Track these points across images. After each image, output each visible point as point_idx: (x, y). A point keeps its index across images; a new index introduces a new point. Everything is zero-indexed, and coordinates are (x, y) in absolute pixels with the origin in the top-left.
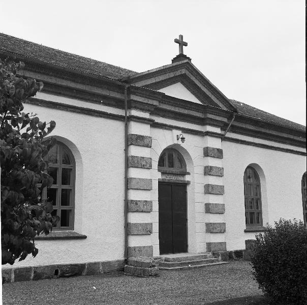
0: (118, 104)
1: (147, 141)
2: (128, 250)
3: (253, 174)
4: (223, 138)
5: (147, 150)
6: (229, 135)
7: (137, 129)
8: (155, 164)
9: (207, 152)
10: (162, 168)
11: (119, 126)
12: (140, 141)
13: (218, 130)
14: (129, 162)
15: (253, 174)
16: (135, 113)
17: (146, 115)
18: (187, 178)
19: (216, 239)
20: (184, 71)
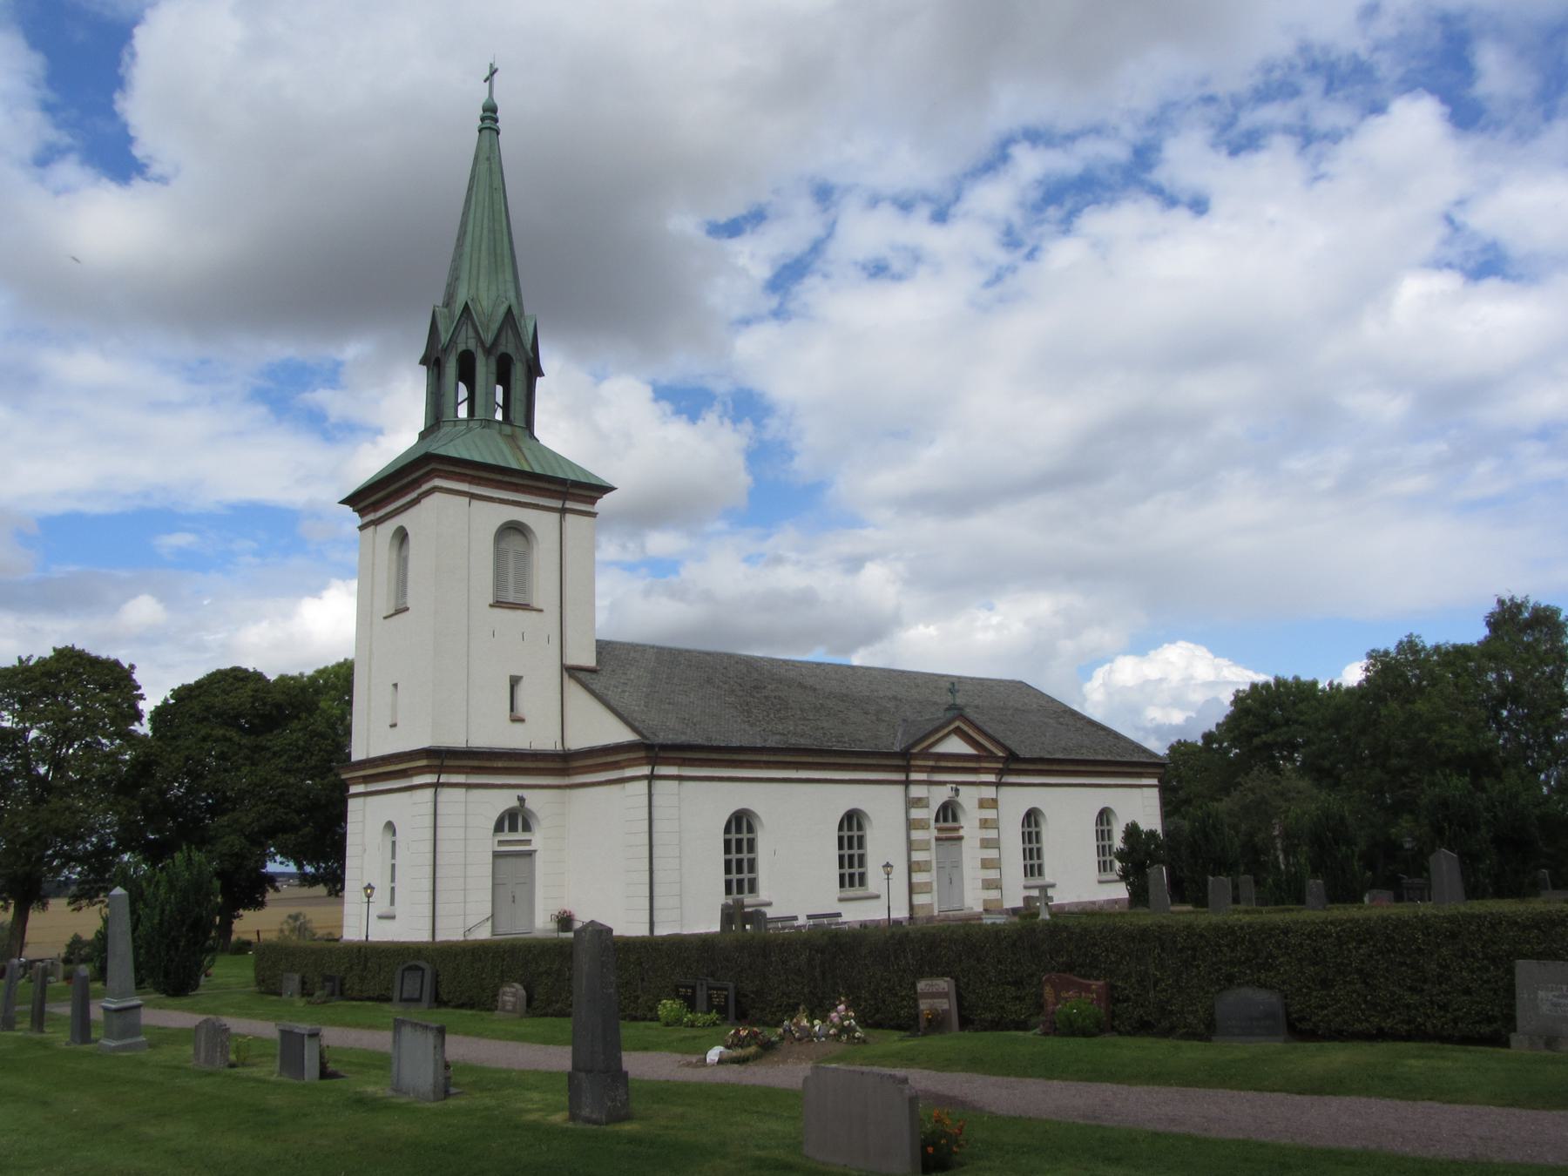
0: (896, 769)
2: (911, 907)
3: (1032, 818)
4: (998, 785)
5: (925, 811)
7: (917, 791)
8: (932, 822)
9: (983, 804)
11: (901, 788)
13: (992, 778)
14: (911, 825)
15: (1032, 818)
16: (914, 776)
18: (962, 833)
19: (993, 894)
20: (957, 723)
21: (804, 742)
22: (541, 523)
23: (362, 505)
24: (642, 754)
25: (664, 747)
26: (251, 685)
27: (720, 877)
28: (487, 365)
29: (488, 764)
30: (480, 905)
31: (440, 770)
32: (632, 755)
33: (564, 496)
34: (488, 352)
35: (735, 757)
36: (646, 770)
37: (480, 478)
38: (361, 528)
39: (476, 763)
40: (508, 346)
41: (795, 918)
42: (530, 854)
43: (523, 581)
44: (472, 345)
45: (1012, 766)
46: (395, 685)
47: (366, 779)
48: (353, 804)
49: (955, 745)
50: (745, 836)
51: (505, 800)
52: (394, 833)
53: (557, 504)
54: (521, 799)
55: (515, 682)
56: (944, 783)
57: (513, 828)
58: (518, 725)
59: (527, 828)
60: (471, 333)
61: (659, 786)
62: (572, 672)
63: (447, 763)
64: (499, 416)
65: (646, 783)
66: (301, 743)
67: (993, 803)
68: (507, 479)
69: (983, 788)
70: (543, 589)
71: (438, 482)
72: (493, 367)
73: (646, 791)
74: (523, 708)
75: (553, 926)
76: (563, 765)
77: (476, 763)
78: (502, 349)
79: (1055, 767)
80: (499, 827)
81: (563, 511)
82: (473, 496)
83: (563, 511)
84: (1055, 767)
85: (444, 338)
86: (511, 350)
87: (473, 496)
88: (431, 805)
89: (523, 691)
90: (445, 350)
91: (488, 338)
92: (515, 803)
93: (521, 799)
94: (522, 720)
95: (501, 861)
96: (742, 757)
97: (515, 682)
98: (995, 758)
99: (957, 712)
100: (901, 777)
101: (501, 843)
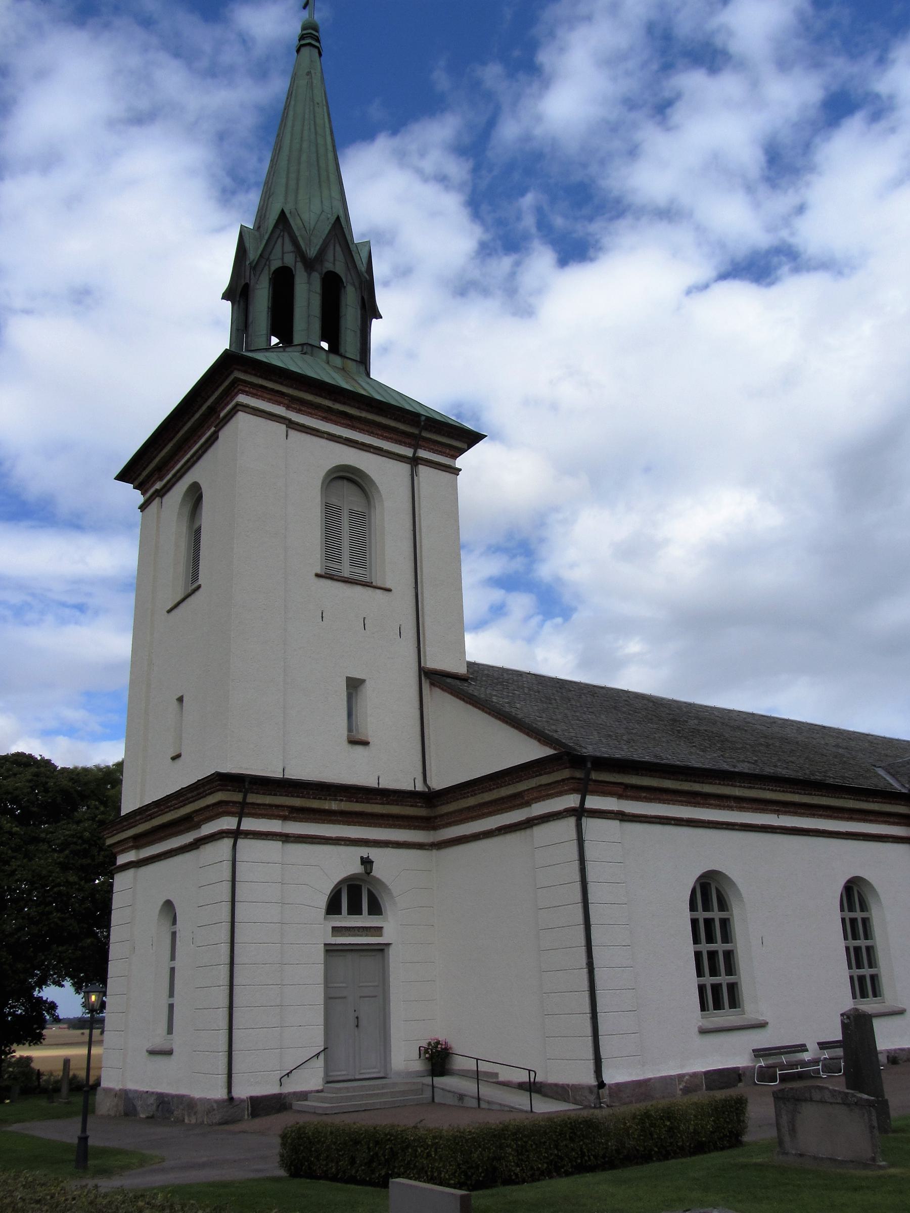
22: (386, 474)
23: (141, 478)
24: (566, 773)
25: (602, 764)
26: (34, 770)
27: (691, 981)
28: (309, 283)
29: (315, 804)
30: (306, 1029)
31: (243, 810)
32: (545, 779)
33: (415, 442)
34: (310, 265)
35: (697, 787)
36: (571, 801)
38: (143, 507)
39: (297, 802)
40: (336, 263)
41: (802, 1048)
42: (382, 949)
44: (290, 260)
46: (180, 700)
47: (139, 841)
48: (122, 882)
50: (716, 915)
51: (342, 863)
52: (174, 922)
54: (367, 862)
55: (354, 685)
57: (355, 909)
58: (359, 749)
59: (375, 908)
60: (289, 247)
61: (591, 825)
62: (434, 678)
63: (252, 798)
65: (571, 821)
66: (87, 834)
71: (242, 398)
72: (317, 285)
73: (573, 835)
74: (371, 727)
75: (418, 1065)
76: (429, 812)
77: (297, 802)
78: (328, 266)
80: (333, 907)
81: (415, 462)
82: (291, 425)
83: (415, 462)
85: (253, 255)
86: (339, 268)
88: (227, 866)
89: (370, 695)
90: (254, 268)
91: (312, 252)
92: (356, 868)
93: (367, 862)
94: (365, 743)
101: (336, 931)
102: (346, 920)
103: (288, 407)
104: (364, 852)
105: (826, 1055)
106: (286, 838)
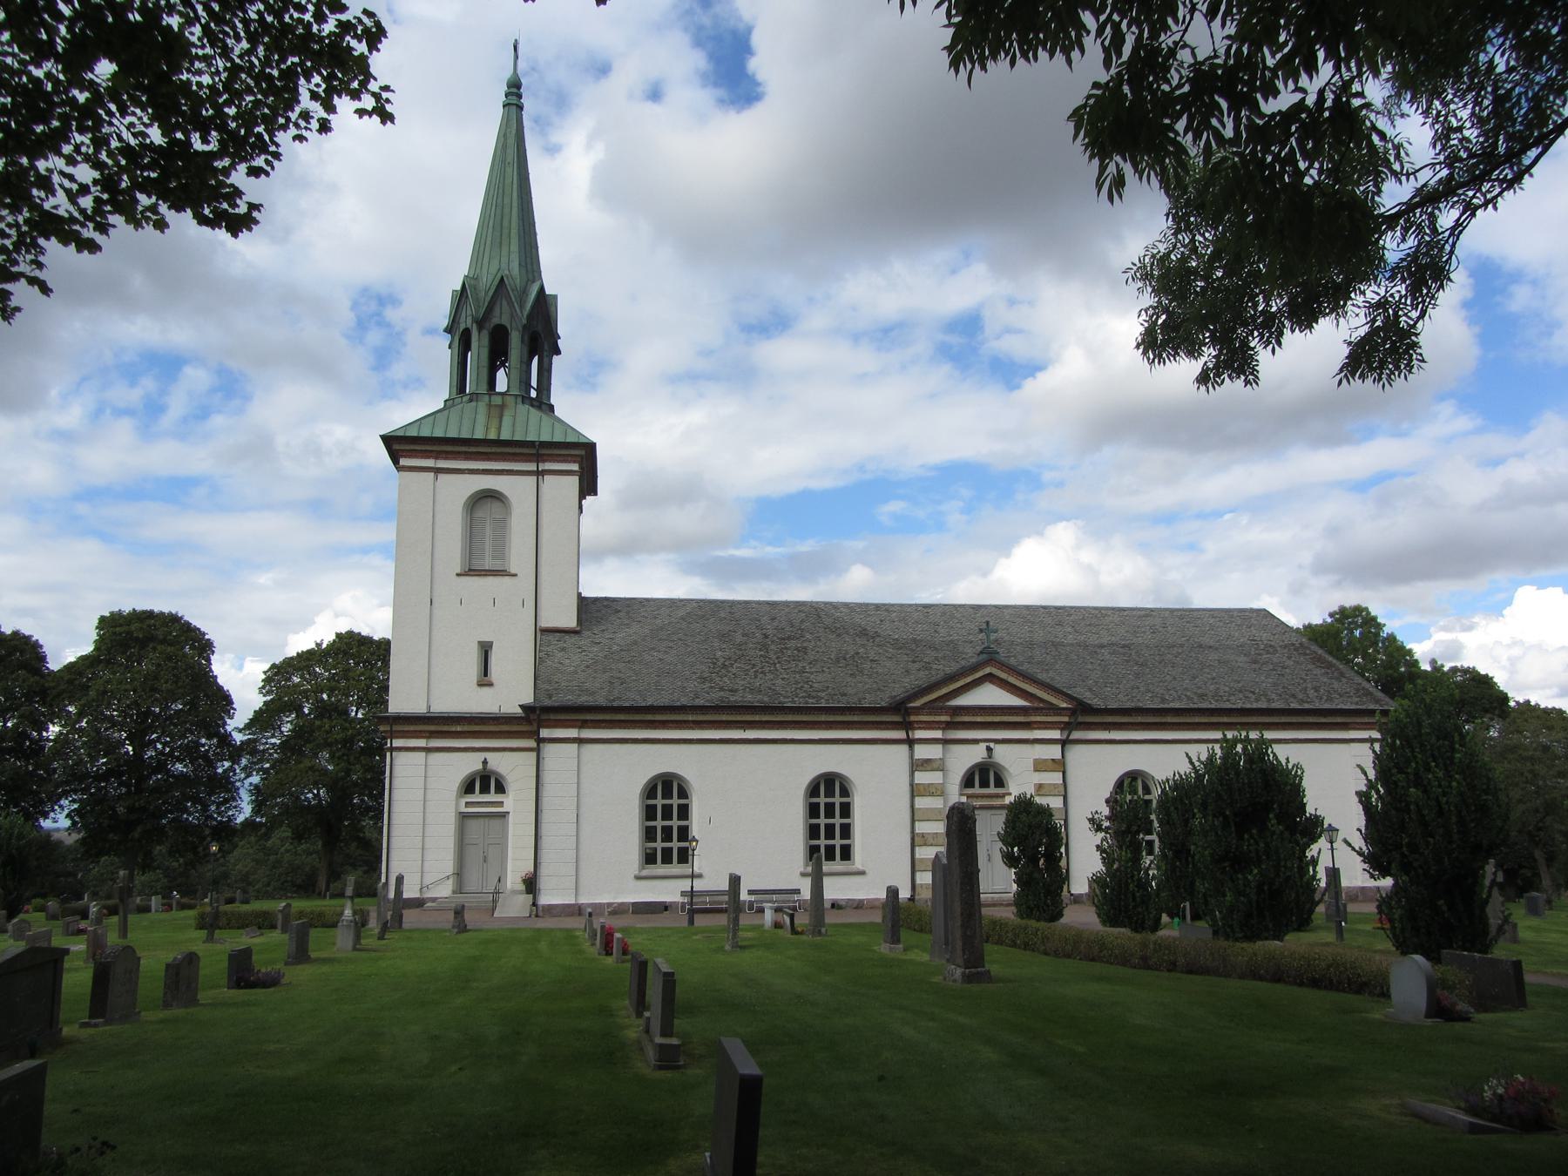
1: (935, 765)
6: (1076, 735)
7: (922, 752)
10: (970, 791)
11: (904, 748)
12: (925, 765)
13: (1056, 734)
14: (915, 791)
16: (919, 734)
17: (938, 734)
20: (988, 670)
21: (750, 698)
22: (516, 487)
29: (446, 728)
30: (442, 861)
37: (447, 452)
39: (432, 728)
42: (504, 815)
43: (501, 549)
45: (1080, 719)
49: (989, 695)
51: (470, 764)
53: (532, 467)
56: (976, 741)
57: (485, 789)
58: (486, 690)
63: (395, 728)
64: (533, 394)
67: (1060, 765)
68: (473, 449)
69: (1038, 747)
70: (519, 555)
77: (432, 728)
78: (495, 321)
79: (1169, 719)
80: (468, 787)
84: (1169, 719)
86: (505, 321)
87: (438, 471)
93: (485, 762)
94: (491, 685)
95: (473, 825)
96: (649, 717)
97: (486, 649)
98: (1058, 711)
99: (989, 656)
100: (901, 735)
101: (468, 804)
102: (477, 797)
103: (436, 458)
104: (481, 756)
105: (753, 898)
106: (428, 750)
